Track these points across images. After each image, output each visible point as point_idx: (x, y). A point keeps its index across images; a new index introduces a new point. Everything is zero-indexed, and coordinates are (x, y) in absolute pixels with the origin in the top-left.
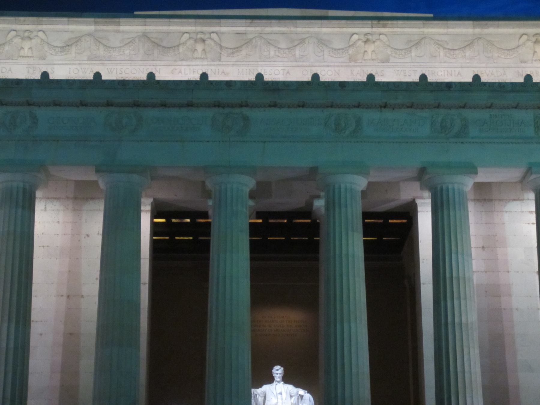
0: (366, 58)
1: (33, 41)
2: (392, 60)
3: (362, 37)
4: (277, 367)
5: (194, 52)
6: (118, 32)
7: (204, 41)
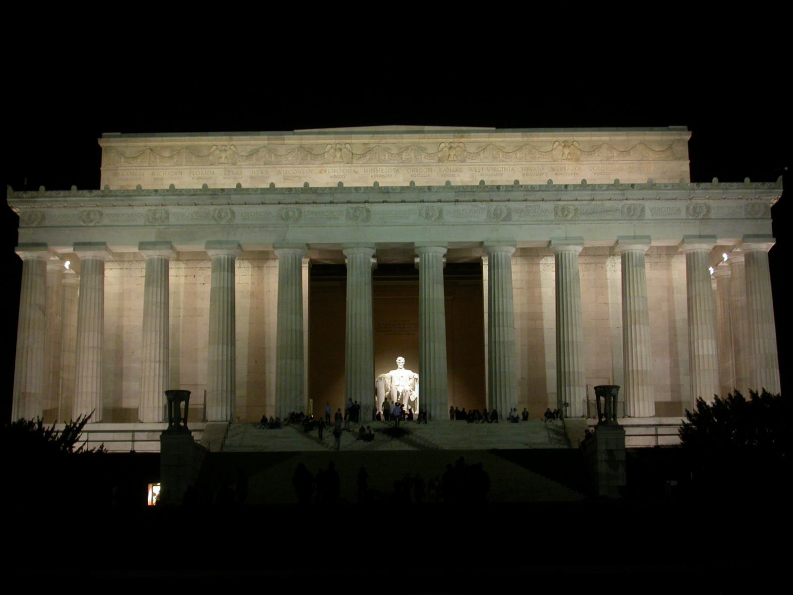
0: (450, 159)
1: (227, 152)
2: (468, 160)
3: (447, 145)
4: (400, 358)
5: (334, 158)
6: (283, 144)
7: (341, 150)
